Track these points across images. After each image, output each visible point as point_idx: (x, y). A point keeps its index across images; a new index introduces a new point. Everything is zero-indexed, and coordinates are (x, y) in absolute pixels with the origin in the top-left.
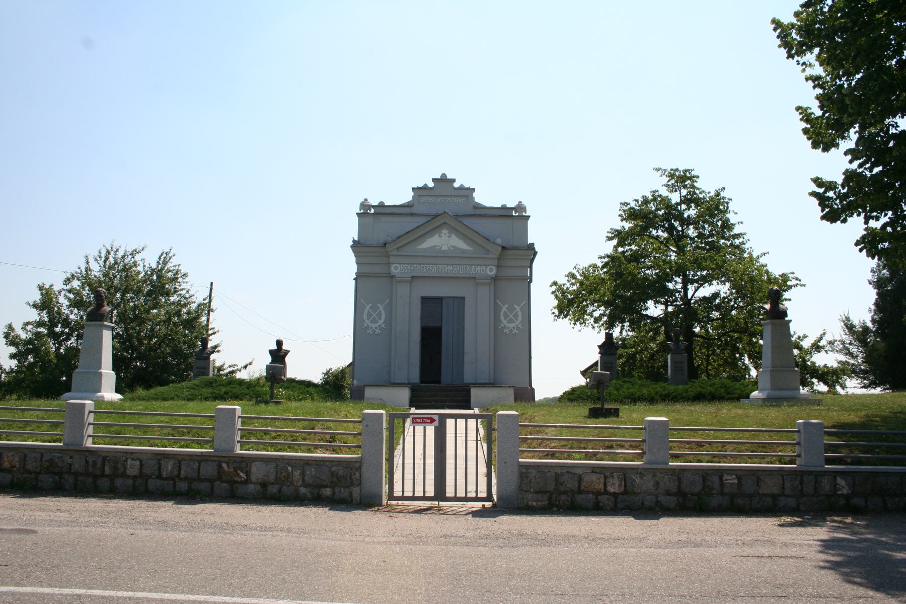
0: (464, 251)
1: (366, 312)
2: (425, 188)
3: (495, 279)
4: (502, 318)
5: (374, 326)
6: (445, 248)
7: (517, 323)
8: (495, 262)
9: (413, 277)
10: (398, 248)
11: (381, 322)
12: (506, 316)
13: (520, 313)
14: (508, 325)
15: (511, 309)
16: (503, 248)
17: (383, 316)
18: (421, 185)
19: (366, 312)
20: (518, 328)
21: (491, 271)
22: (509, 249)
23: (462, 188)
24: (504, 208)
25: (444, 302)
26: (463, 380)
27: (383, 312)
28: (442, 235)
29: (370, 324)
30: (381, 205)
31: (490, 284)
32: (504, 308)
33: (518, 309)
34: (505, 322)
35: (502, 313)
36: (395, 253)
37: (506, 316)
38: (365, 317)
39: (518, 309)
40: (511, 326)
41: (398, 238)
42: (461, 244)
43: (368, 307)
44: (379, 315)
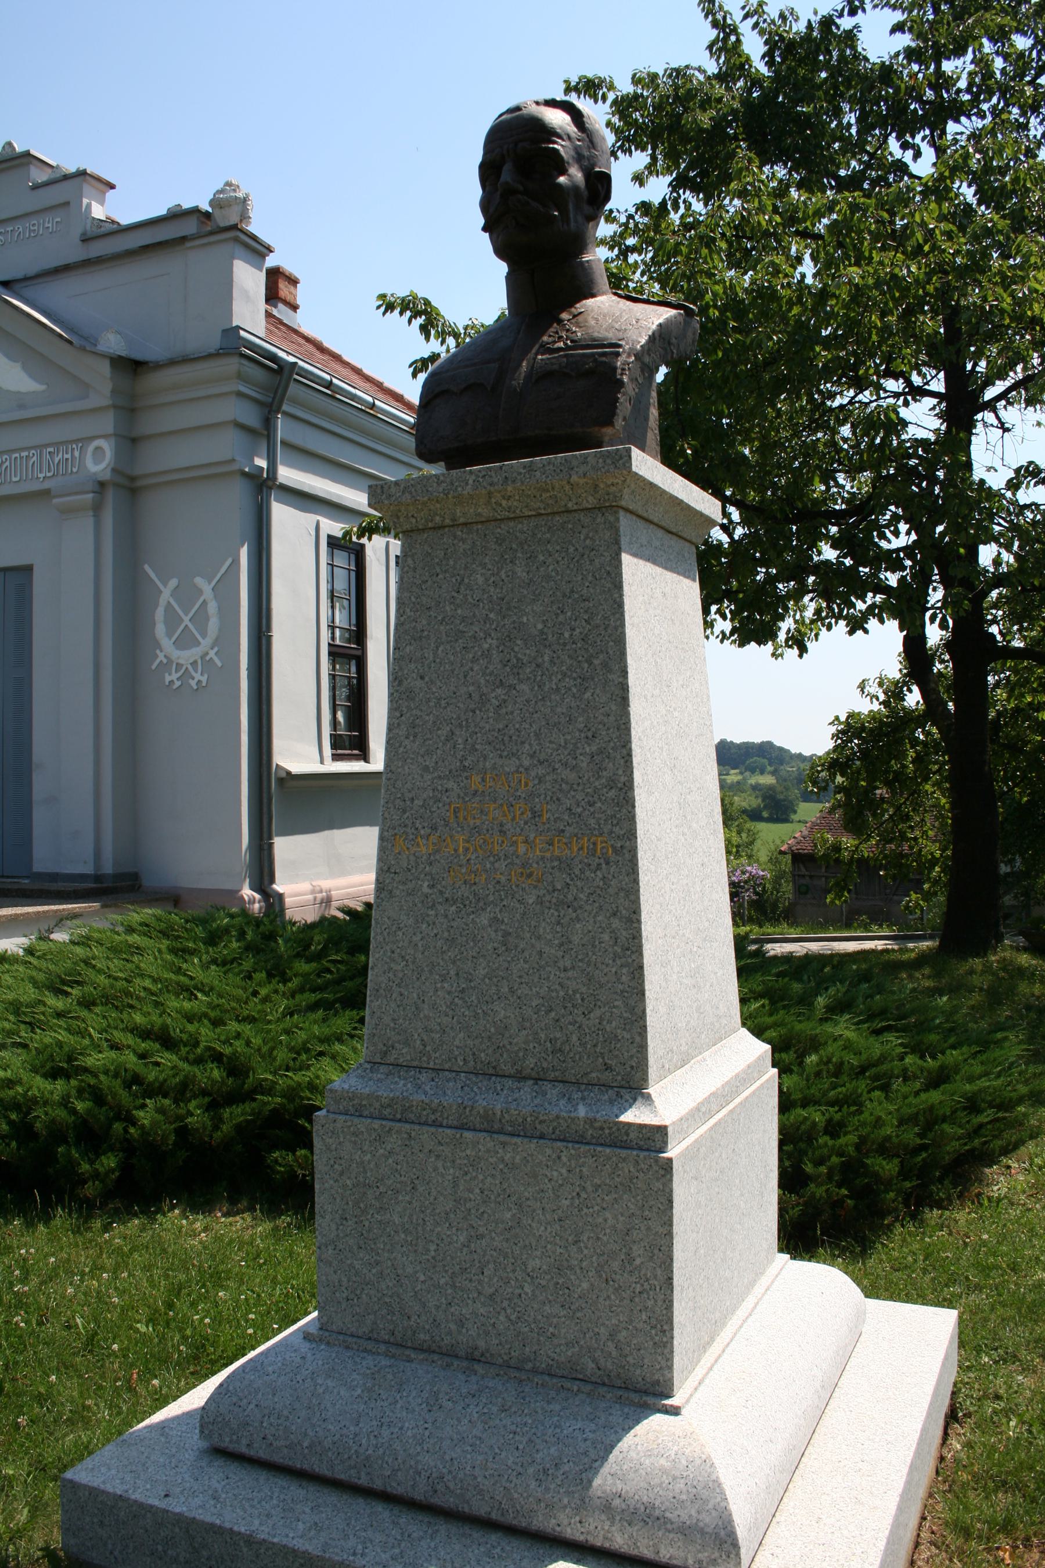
0: (21, 400)
4: (160, 630)
7: (205, 643)
8: (107, 423)
12: (172, 620)
13: (212, 607)
14: (176, 654)
15: (187, 594)
16: (131, 367)
20: (207, 663)
21: (98, 460)
22: (158, 366)
24: (176, 215)
26: (31, 866)
31: (97, 508)
32: (166, 596)
33: (207, 589)
35: (160, 614)
37: (172, 620)
39: (207, 589)
40: (185, 657)
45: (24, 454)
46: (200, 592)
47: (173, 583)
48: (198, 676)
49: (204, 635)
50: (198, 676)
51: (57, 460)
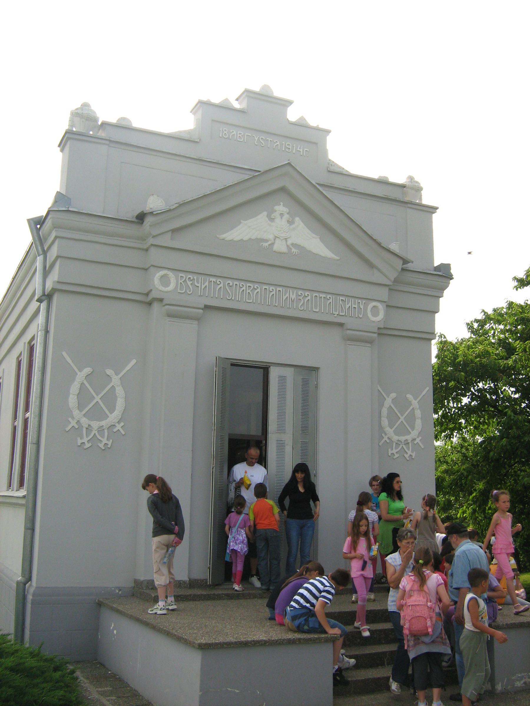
1: (75, 388)
2: (225, 107)
3: (384, 332)
5: (95, 425)
6: (280, 246)
7: (414, 434)
9: (207, 307)
10: (175, 231)
11: (114, 417)
17: (120, 403)
18: (217, 100)
19: (75, 388)
21: (376, 316)
23: (301, 124)
24: (383, 182)
25: (274, 374)
27: (120, 391)
28: (276, 215)
29: (85, 422)
30: (123, 126)
34: (390, 431)
36: (166, 240)
37: (392, 417)
38: (72, 401)
39: (415, 403)
41: (182, 205)
42: (316, 245)
43: (81, 376)
44: (110, 400)
45: (323, 296)
46: (410, 404)
47: (393, 395)
48: (409, 453)
49: (413, 428)
50: (409, 453)
51: (347, 306)
